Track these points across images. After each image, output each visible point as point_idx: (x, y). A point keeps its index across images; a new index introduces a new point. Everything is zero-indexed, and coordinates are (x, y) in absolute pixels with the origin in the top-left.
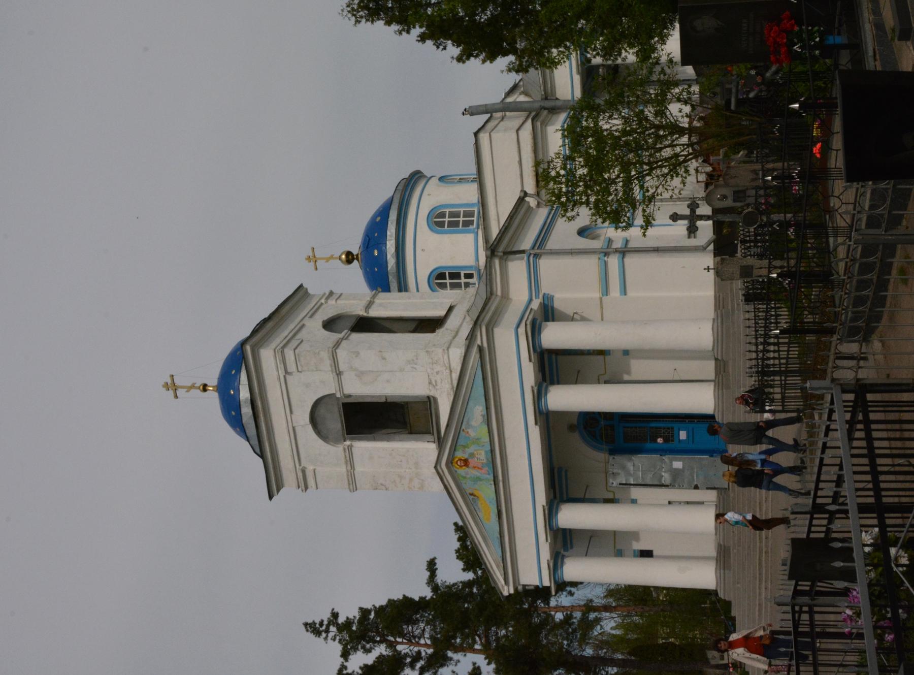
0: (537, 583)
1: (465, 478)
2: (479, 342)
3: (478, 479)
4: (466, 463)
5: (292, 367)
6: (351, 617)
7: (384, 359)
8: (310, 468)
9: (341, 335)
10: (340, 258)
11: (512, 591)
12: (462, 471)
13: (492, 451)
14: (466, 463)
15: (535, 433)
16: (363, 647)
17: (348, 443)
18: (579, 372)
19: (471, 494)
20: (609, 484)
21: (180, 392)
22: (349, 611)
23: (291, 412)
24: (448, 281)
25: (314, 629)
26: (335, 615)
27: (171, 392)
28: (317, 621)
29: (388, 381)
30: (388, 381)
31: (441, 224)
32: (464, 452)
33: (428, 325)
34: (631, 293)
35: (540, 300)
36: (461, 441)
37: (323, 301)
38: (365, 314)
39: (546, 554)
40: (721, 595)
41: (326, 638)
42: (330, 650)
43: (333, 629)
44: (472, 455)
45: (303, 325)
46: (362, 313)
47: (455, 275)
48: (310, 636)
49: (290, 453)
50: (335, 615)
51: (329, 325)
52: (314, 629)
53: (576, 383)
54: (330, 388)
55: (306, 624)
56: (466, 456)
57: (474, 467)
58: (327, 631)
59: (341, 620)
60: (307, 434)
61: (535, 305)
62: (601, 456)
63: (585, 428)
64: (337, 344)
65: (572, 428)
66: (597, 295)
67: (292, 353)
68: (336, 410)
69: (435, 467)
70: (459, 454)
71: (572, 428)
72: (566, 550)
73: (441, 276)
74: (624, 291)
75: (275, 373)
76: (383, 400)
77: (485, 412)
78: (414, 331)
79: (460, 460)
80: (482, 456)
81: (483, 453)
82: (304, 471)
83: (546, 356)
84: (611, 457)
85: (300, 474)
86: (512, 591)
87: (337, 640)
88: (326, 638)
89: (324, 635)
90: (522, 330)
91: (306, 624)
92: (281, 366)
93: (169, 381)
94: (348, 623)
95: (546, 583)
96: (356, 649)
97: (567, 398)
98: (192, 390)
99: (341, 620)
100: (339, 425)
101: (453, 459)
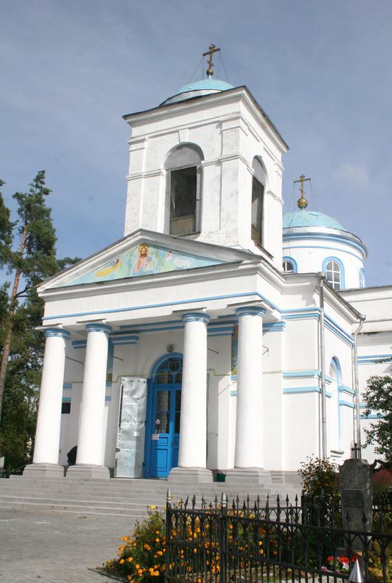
0: (46, 315)
1: (131, 255)
2: (244, 262)
3: (130, 266)
4: (144, 255)
5: (225, 126)
6: (45, 203)
7: (231, 196)
8: (146, 144)
9: (250, 166)
11: (40, 295)
12: (137, 251)
13: (152, 276)
15: (167, 312)
16: (22, 210)
17: (164, 172)
18: (218, 353)
19: (118, 261)
20: (123, 378)
21: (208, 57)
22: (48, 201)
23: (190, 128)
25: (40, 178)
26: (46, 192)
27: (208, 50)
29: (213, 200)
30: (213, 200)
32: (152, 253)
33: (257, 233)
34: (285, 397)
35: (280, 319)
36: (161, 252)
37: (276, 161)
38: (266, 191)
40: (28, 467)
41: (32, 185)
42: (26, 187)
43: (38, 191)
44: (150, 260)
45: (259, 141)
46: (266, 189)
50: (46, 192)
52: (40, 178)
53: (208, 349)
54: (208, 157)
55: (43, 172)
56: (149, 255)
57: (140, 262)
59: (44, 197)
60: (173, 141)
61: (276, 314)
62: (147, 372)
63: (170, 359)
64: (244, 161)
65: (171, 348)
66: (285, 367)
68: (191, 163)
69: (141, 230)
70: (151, 250)
71: (171, 348)
72: (74, 343)
74: (288, 392)
75: (221, 114)
77: (185, 268)
78: (253, 226)
79: (146, 251)
80: (149, 268)
81: (152, 268)
82: (143, 141)
83: (232, 325)
84: (145, 380)
85: (141, 138)
86: (40, 295)
87: (31, 193)
88: (32, 185)
89: (35, 184)
90: (258, 298)
91: (43, 172)
92: (227, 118)
93: (215, 48)
94: (40, 201)
95: (45, 323)
96: (21, 203)
97: (196, 337)
98: (208, 65)
99: (44, 197)
101: (147, 246)
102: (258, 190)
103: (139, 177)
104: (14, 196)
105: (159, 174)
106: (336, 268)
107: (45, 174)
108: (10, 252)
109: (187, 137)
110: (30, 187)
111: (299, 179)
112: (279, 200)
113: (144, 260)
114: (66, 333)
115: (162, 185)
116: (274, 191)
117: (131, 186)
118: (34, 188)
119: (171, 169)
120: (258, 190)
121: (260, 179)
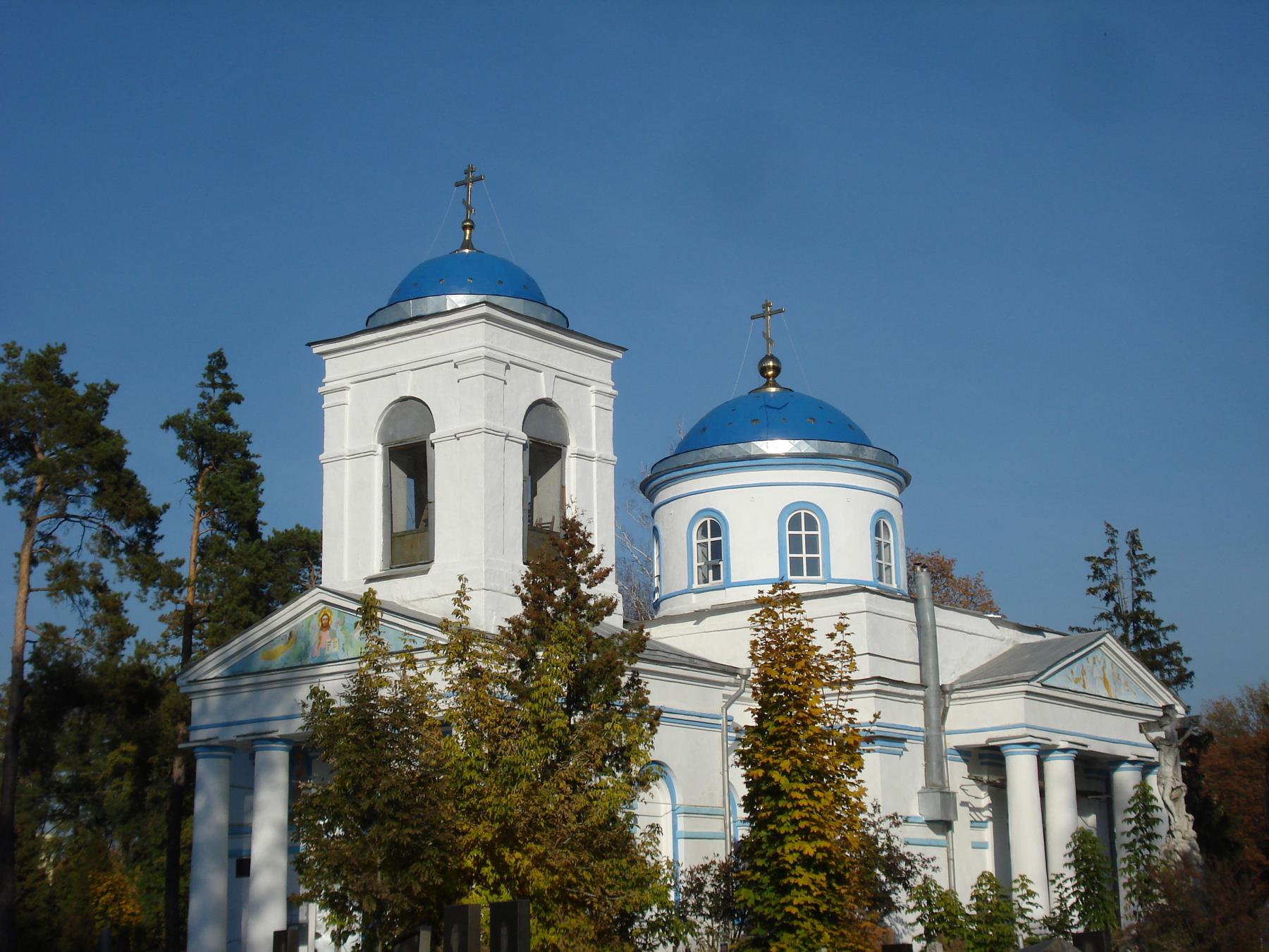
5: (463, 371)
8: (348, 396)
10: (768, 358)
14: (325, 627)
17: (380, 449)
24: (709, 540)
26: (238, 399)
28: (227, 370)
31: (795, 524)
38: (568, 454)
39: (232, 734)
44: (334, 635)
46: (571, 449)
47: (717, 550)
48: (205, 362)
49: (365, 369)
50: (238, 399)
51: (542, 409)
56: (332, 626)
58: (214, 386)
67: (483, 371)
73: (716, 530)
76: (430, 499)
82: (343, 389)
94: (228, 422)
96: (182, 436)
99: (233, 409)
100: (399, 438)
102: (543, 455)
103: (339, 458)
104: (167, 425)
105: (371, 453)
106: (811, 524)
107: (227, 355)
108: (158, 567)
109: (408, 386)
110: (200, 390)
111: (760, 311)
112: (602, 460)
113: (326, 635)
114: (228, 749)
115: (377, 465)
116: (593, 449)
117: (328, 471)
118: (210, 390)
119: (389, 443)
120: (543, 455)
121: (550, 437)
